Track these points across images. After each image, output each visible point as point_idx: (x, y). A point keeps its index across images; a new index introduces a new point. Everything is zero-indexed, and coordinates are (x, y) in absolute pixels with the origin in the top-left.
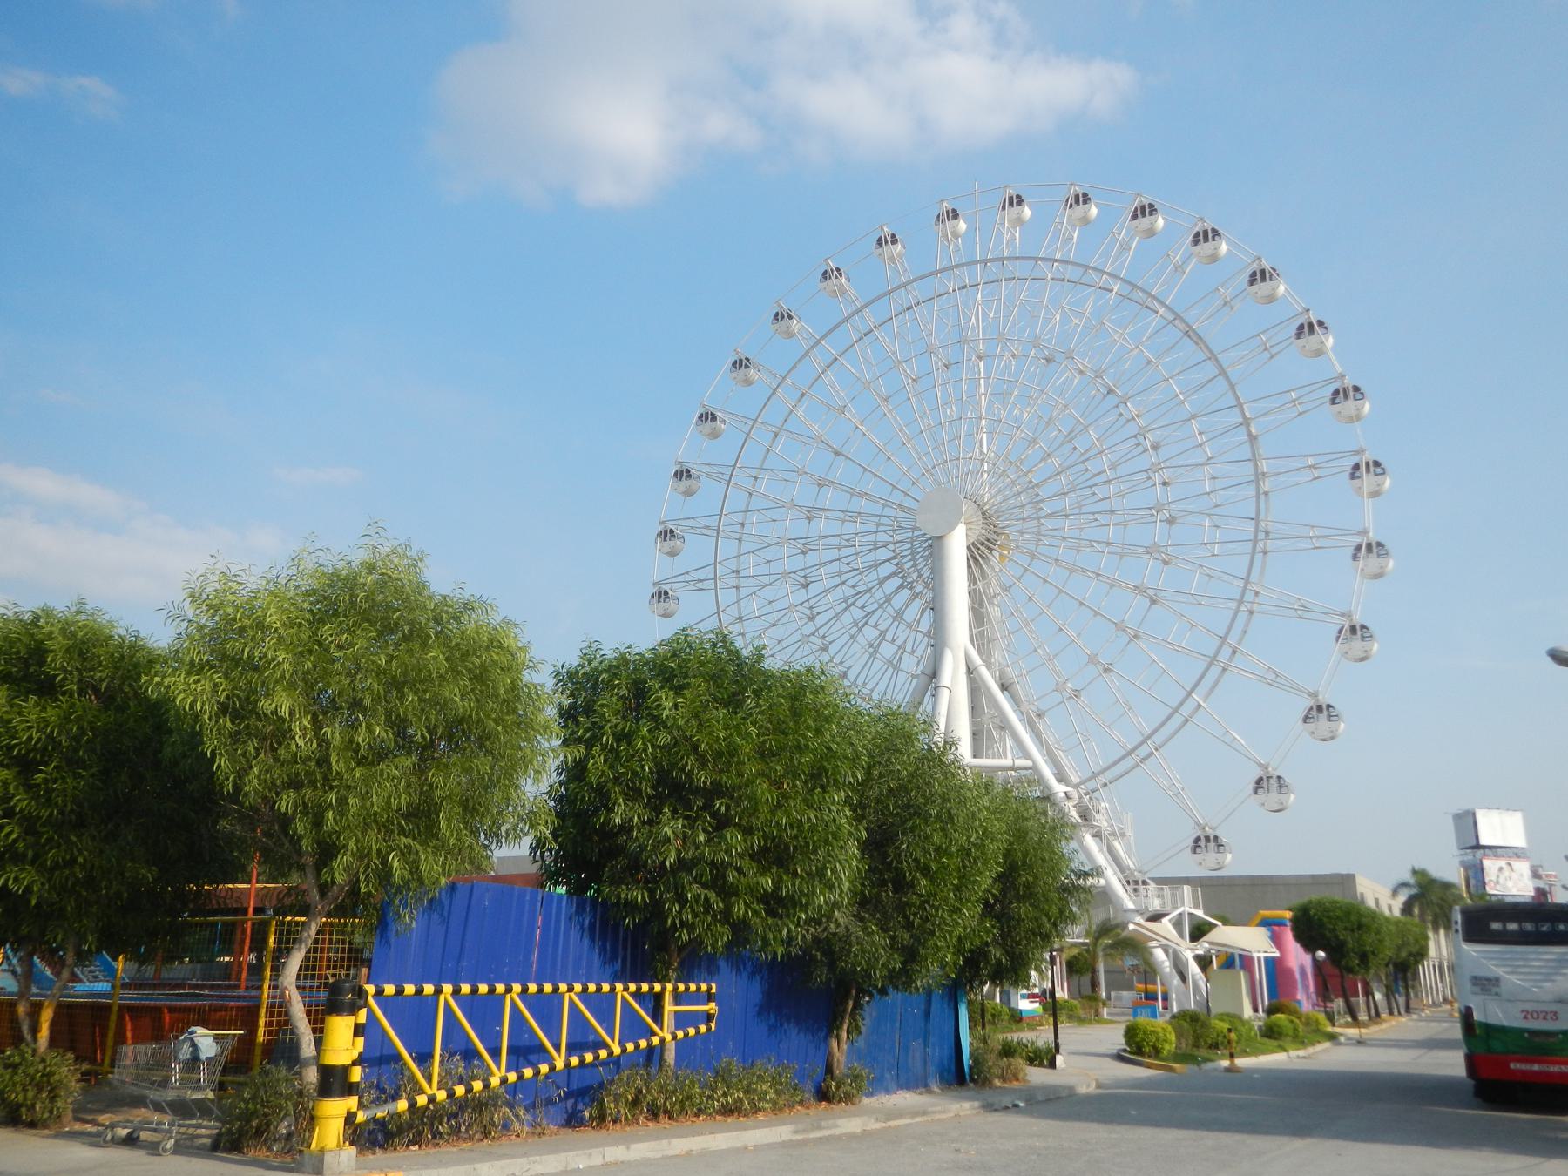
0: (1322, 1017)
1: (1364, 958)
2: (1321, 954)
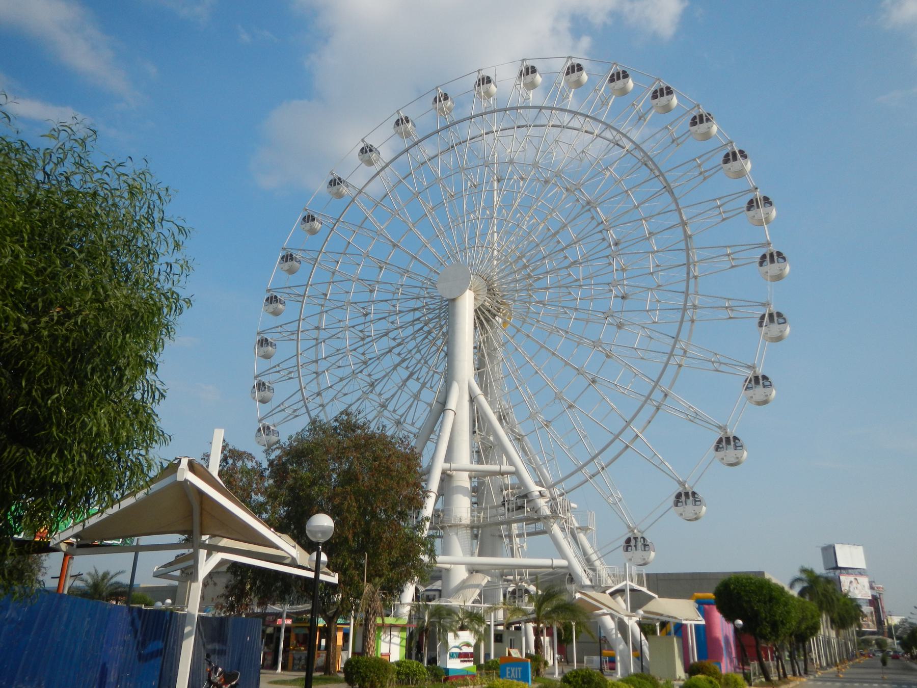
0: (740, 677)
1: (774, 626)
2: (740, 622)
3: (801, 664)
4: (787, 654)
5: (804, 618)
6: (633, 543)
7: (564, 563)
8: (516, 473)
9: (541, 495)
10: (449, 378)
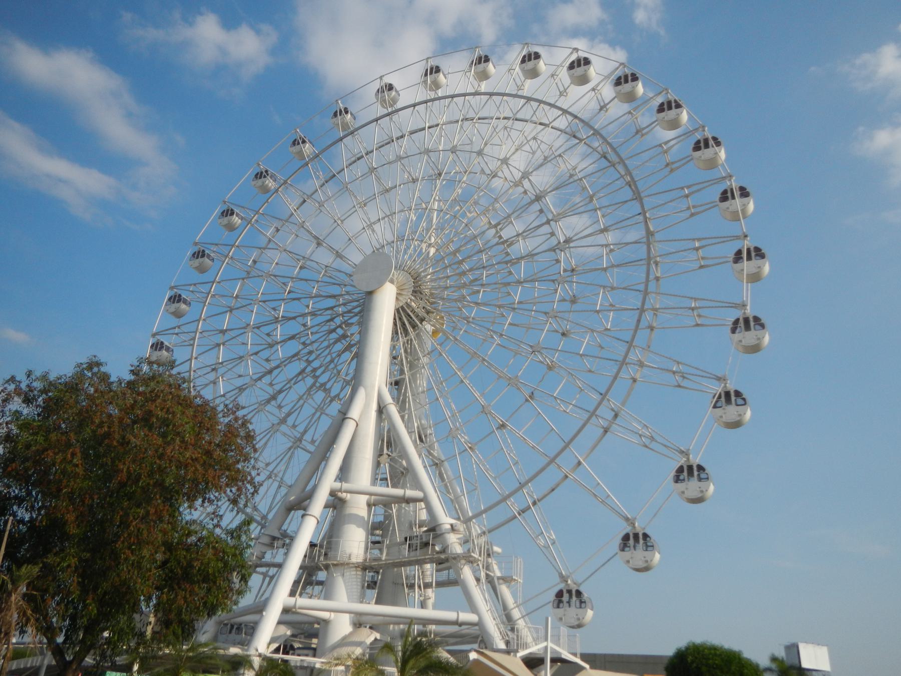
10: (355, 381)
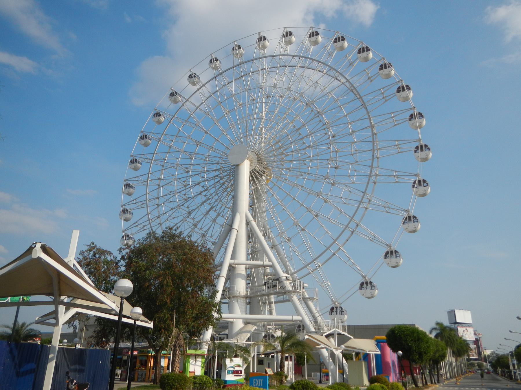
0: (400, 385)
1: (420, 355)
2: (400, 352)
3: (436, 377)
4: (428, 371)
5: (438, 351)
6: (335, 310)
7: (299, 318)
8: (272, 266)
9: (287, 279)
